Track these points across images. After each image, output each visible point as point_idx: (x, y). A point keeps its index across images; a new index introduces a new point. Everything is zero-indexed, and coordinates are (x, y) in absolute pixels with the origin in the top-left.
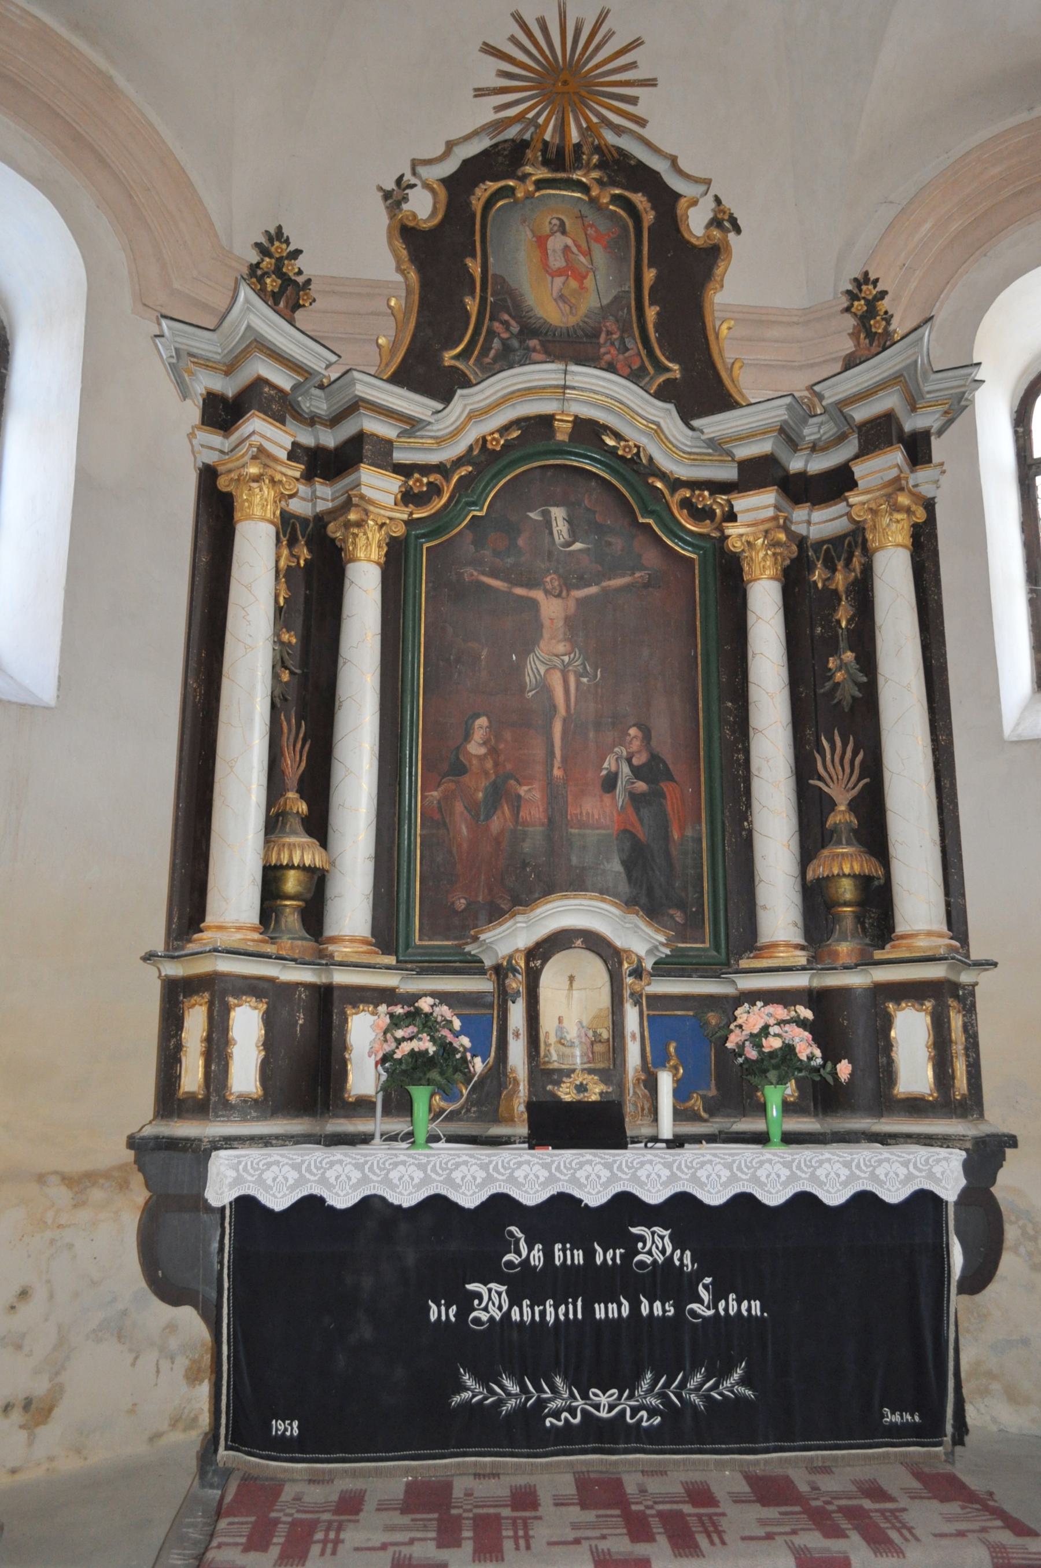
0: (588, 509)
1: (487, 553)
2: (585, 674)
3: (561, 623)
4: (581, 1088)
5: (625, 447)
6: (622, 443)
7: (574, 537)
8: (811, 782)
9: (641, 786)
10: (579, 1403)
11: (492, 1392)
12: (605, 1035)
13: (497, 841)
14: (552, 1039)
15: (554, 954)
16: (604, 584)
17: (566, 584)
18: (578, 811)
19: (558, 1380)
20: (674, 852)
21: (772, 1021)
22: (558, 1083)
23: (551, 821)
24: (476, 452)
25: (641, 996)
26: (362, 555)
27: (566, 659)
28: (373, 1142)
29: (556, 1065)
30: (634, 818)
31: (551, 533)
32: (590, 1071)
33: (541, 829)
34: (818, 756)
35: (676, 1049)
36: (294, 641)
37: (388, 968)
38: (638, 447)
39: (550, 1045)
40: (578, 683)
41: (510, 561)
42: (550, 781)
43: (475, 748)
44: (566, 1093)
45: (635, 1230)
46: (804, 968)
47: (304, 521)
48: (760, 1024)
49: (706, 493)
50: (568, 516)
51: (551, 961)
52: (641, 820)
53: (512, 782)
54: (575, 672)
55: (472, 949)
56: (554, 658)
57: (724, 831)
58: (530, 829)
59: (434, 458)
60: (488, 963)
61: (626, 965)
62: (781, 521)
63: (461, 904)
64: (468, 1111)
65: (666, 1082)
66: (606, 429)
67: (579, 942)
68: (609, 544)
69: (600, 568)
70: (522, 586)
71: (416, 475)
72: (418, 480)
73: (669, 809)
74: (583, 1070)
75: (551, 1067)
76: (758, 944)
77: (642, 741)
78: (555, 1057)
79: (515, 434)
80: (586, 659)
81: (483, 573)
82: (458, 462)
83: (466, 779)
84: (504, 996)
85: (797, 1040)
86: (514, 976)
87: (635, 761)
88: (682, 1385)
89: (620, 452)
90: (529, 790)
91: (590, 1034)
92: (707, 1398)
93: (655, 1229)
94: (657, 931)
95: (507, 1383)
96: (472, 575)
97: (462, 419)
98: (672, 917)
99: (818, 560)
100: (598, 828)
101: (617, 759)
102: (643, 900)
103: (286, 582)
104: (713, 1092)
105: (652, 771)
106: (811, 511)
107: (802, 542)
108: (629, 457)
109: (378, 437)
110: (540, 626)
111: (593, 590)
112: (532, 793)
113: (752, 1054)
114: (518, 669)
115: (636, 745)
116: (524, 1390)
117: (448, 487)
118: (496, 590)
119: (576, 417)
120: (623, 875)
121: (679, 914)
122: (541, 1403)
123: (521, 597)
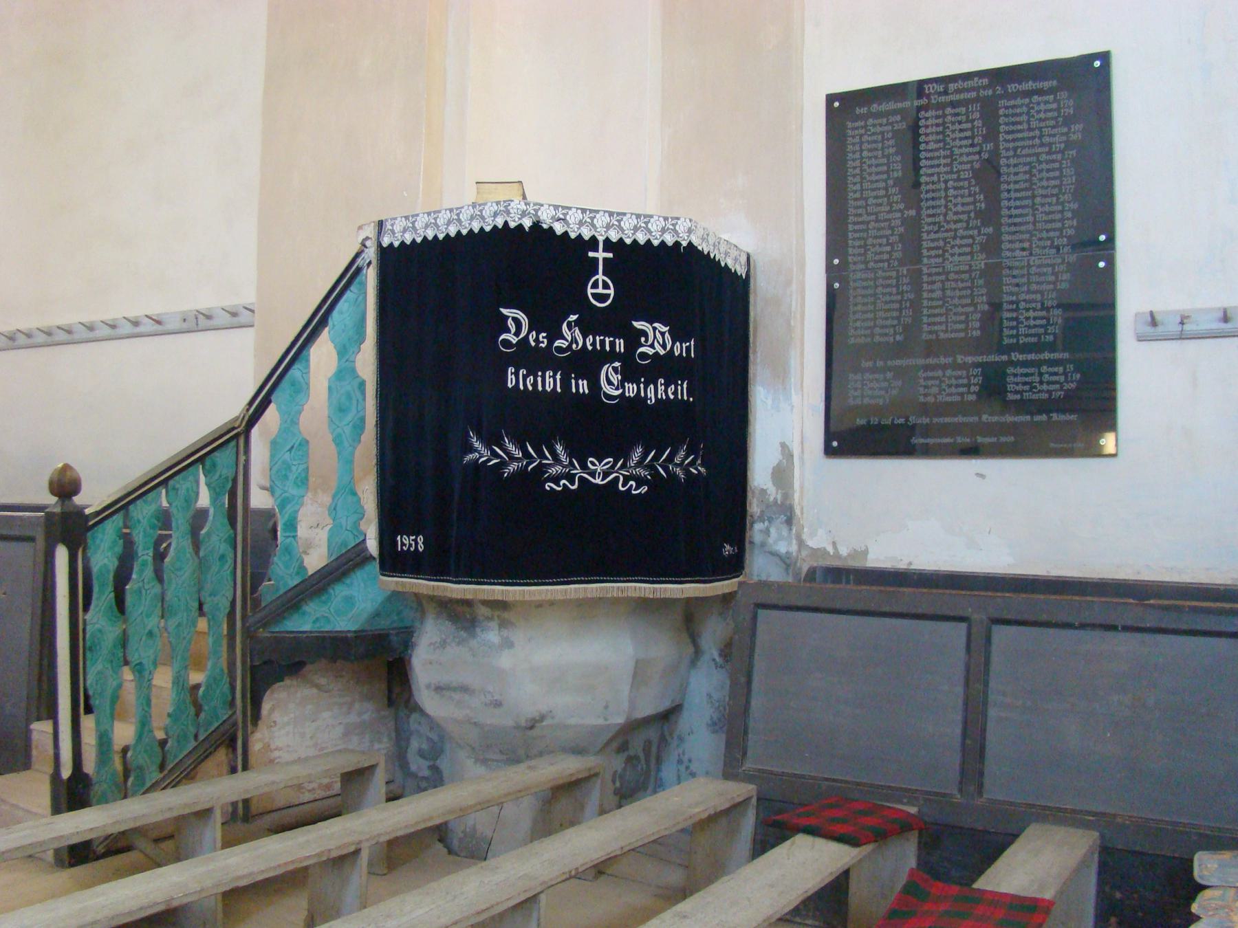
10: (578, 471)
11: (496, 455)
19: (559, 448)
45: (636, 324)
88: (670, 459)
92: (688, 473)
93: (656, 325)
95: (511, 447)
116: (526, 454)
122: (541, 468)
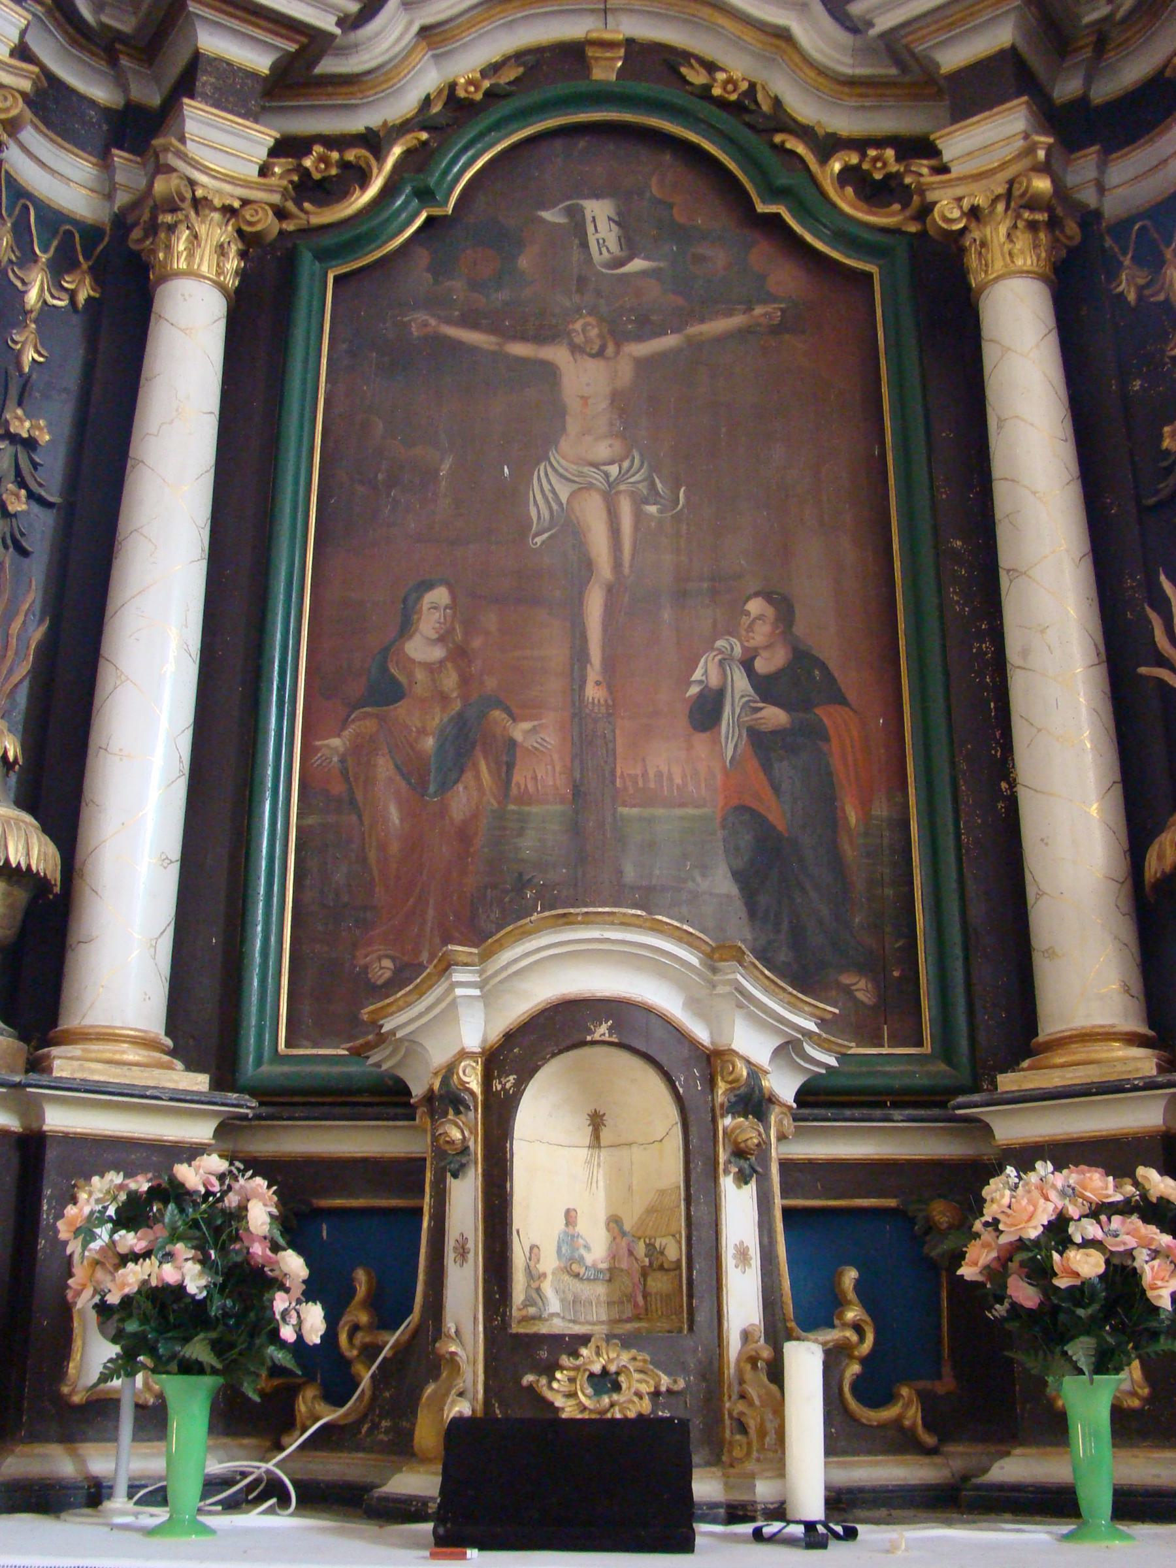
0: (660, 201)
1: (457, 287)
2: (653, 496)
3: (604, 404)
4: (606, 1381)
5: (729, 81)
6: (720, 76)
7: (631, 246)
8: (1143, 670)
9: (774, 716)
12: (674, 1251)
13: (464, 835)
14: (549, 1262)
15: (546, 1061)
16: (694, 330)
17: (612, 333)
18: (639, 771)
20: (850, 852)
21: (1073, 1211)
22: (549, 1369)
23: (578, 793)
24: (436, 109)
25: (764, 1158)
26: (183, 265)
27: (614, 470)
28: (108, 1505)
29: (557, 1326)
30: (758, 779)
31: (585, 245)
32: (627, 1342)
33: (558, 808)
34: (1153, 616)
35: (859, 1286)
36: (45, 438)
37: (179, 1097)
38: (752, 86)
39: (545, 1275)
40: (638, 516)
41: (503, 295)
42: (578, 711)
43: (422, 648)
44: (568, 1396)
46: (1150, 1085)
47: (91, 233)
48: (1045, 1215)
49: (890, 153)
50: (618, 214)
51: (539, 1076)
52: (776, 789)
53: (497, 714)
54: (633, 495)
55: (382, 1060)
56: (586, 469)
57: (955, 800)
58: (535, 809)
59: (357, 123)
60: (418, 1090)
61: (722, 1087)
62: (1041, 154)
63: (383, 969)
64: (375, 1426)
65: (805, 1363)
66: (687, 56)
67: (602, 1031)
68: (700, 259)
69: (680, 301)
70: (524, 338)
71: (318, 149)
72: (322, 159)
73: (836, 762)
74: (609, 1338)
75: (544, 1329)
76: (1042, 1037)
77: (775, 626)
78: (554, 1305)
79: (511, 74)
80: (655, 468)
81: (449, 321)
82: (404, 128)
83: (400, 710)
84: (451, 1162)
85: (1142, 1255)
86: (458, 1112)
87: (760, 666)
89: (717, 91)
90: (534, 730)
91: (641, 1249)
94: (793, 1006)
96: (425, 325)
97: (404, 43)
98: (847, 991)
99: (1125, 254)
100: (682, 805)
101: (721, 663)
102: (784, 955)
103: (39, 331)
104: (946, 1385)
105: (797, 683)
106: (1102, 166)
107: (1090, 218)
108: (733, 97)
109: (229, 64)
110: (559, 413)
111: (670, 341)
112: (541, 739)
113: (1024, 1293)
114: (512, 496)
115: (761, 634)
117: (380, 170)
118: (473, 350)
119: (630, 42)
120: (738, 908)
121: (862, 984)
123: (523, 361)
